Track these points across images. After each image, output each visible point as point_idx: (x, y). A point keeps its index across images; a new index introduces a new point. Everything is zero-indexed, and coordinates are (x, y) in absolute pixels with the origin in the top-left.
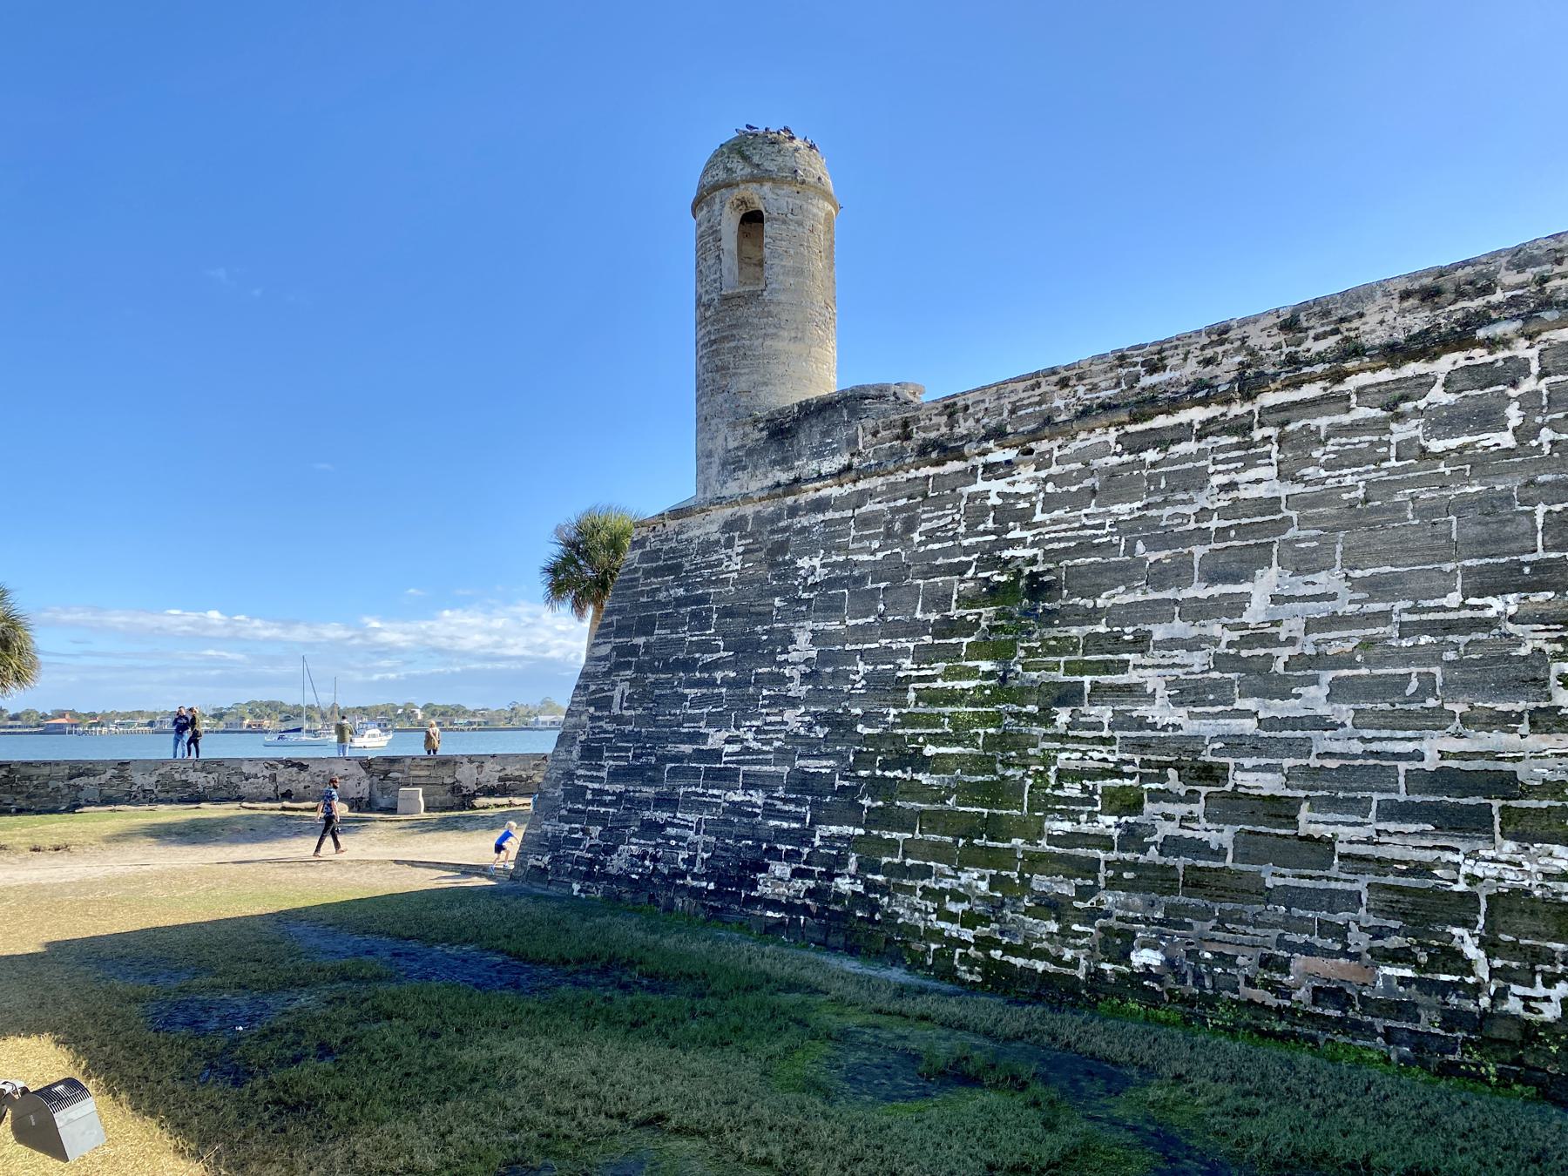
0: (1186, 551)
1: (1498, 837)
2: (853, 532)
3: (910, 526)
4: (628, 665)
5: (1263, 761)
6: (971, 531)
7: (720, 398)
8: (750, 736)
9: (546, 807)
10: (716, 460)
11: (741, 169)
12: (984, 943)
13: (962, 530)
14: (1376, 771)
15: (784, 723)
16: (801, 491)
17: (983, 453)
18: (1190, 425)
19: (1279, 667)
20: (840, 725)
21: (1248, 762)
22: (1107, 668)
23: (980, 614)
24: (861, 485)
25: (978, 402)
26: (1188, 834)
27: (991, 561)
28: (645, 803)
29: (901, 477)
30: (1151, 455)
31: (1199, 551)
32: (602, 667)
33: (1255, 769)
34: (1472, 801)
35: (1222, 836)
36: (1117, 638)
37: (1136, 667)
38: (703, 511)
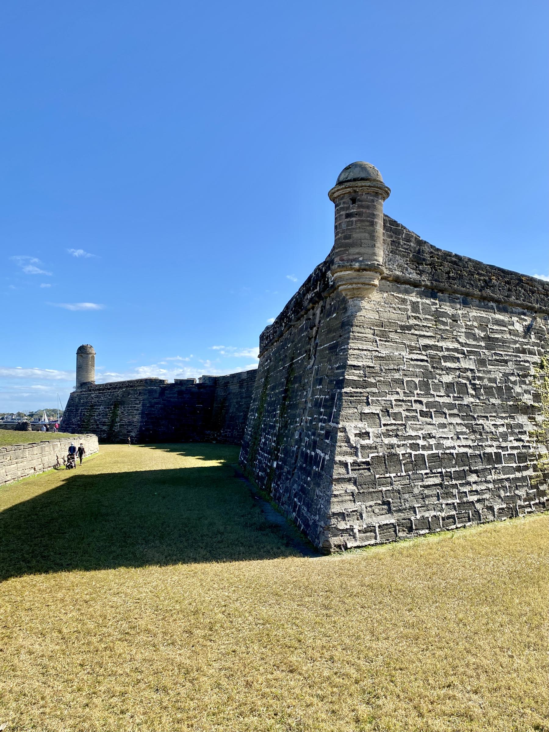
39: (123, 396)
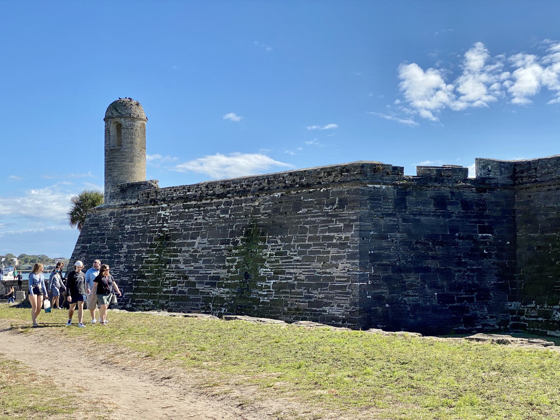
4: (84, 252)
7: (110, 178)
10: (108, 195)
11: (116, 114)
17: (162, 204)
20: (130, 268)
21: (191, 275)
24: (139, 208)
27: (161, 231)
29: (147, 207)
30: (187, 210)
31: (191, 232)
32: (78, 252)
35: (186, 290)
39: (276, 211)
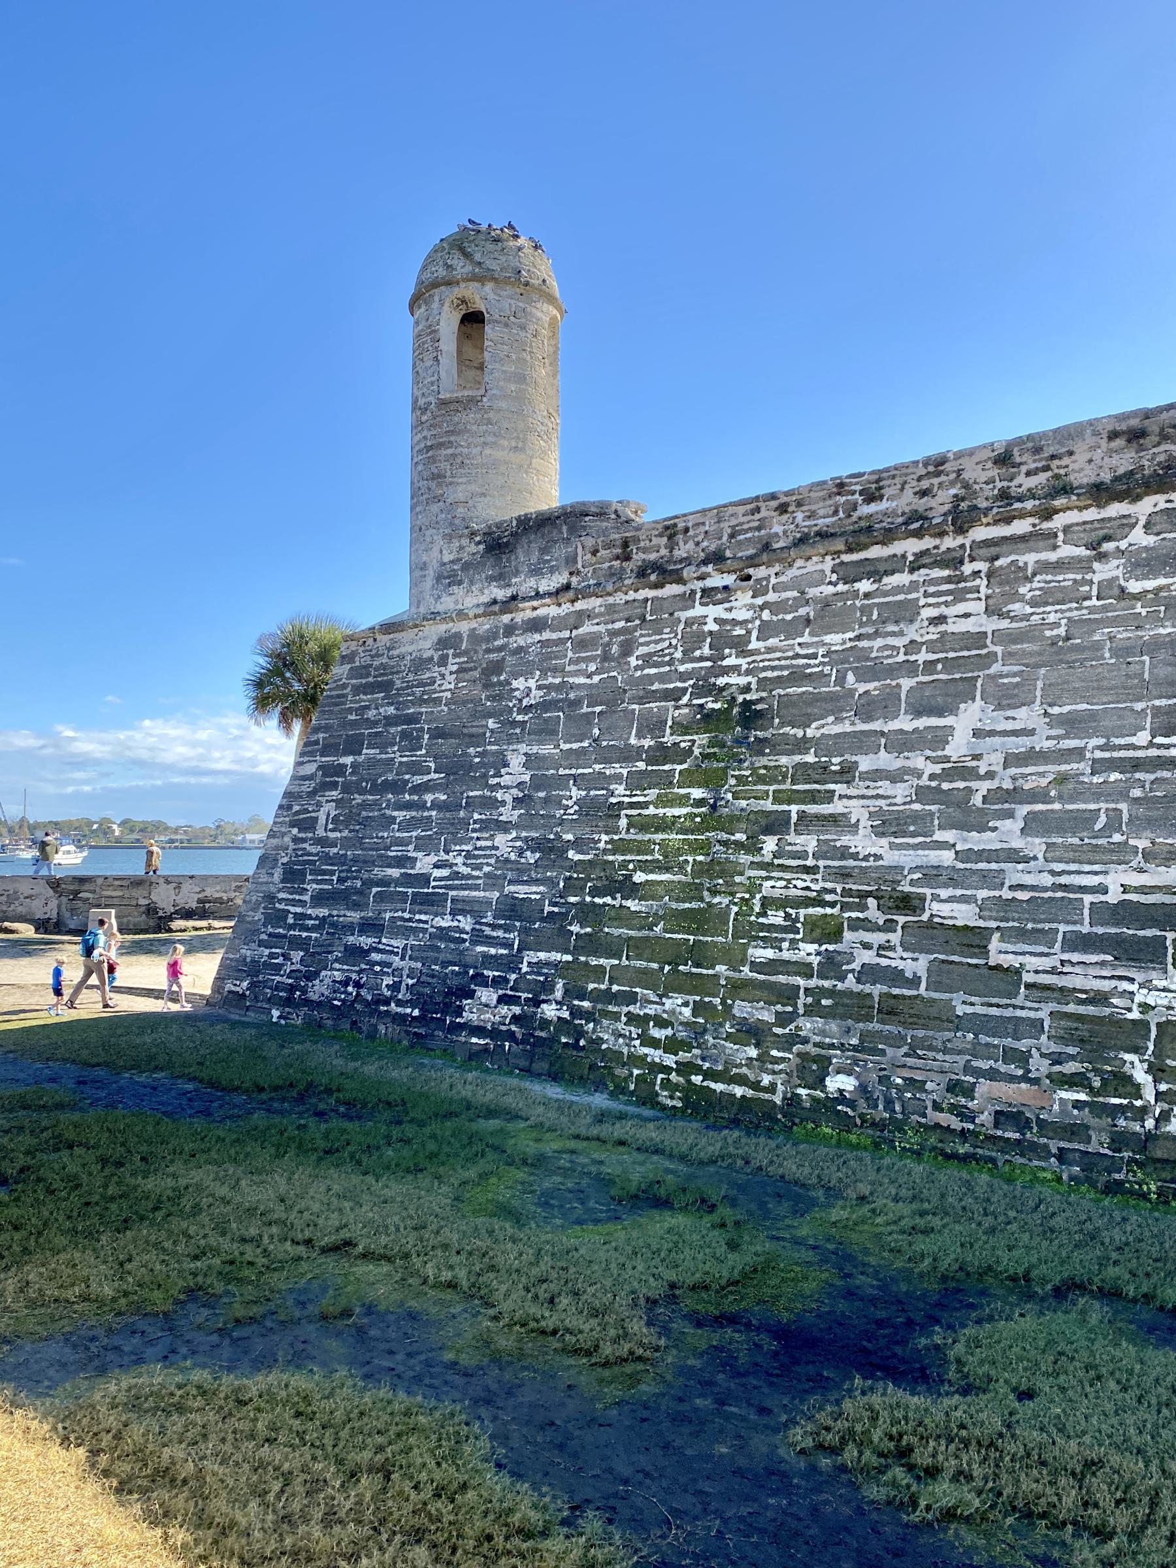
0: (894, 683)
1: (1170, 967)
2: (570, 654)
3: (627, 649)
4: (334, 785)
5: (959, 892)
6: (687, 657)
7: (435, 508)
8: (460, 860)
9: (245, 933)
10: (430, 573)
11: (461, 267)
12: (685, 1068)
13: (678, 655)
14: (1060, 903)
15: (497, 848)
16: (517, 610)
17: (702, 578)
18: (904, 556)
19: (977, 800)
20: (551, 850)
21: (944, 893)
22: (813, 797)
23: (694, 741)
25: (698, 525)
26: (884, 962)
27: (706, 688)
28: (349, 928)
29: (620, 598)
30: (865, 586)
31: (906, 683)
32: (308, 786)
33: (950, 900)
34: (1148, 933)
35: (917, 965)
36: (825, 768)
37: (841, 797)
38: (416, 626)
